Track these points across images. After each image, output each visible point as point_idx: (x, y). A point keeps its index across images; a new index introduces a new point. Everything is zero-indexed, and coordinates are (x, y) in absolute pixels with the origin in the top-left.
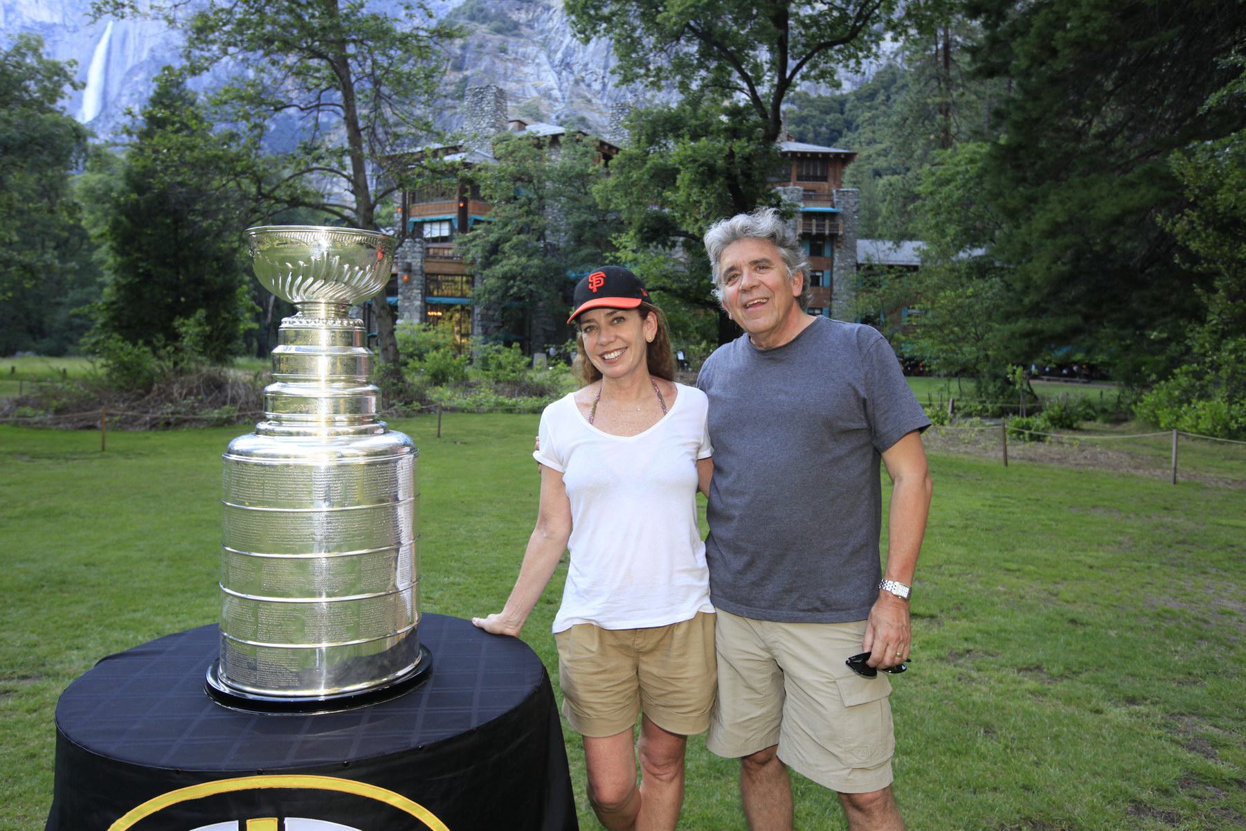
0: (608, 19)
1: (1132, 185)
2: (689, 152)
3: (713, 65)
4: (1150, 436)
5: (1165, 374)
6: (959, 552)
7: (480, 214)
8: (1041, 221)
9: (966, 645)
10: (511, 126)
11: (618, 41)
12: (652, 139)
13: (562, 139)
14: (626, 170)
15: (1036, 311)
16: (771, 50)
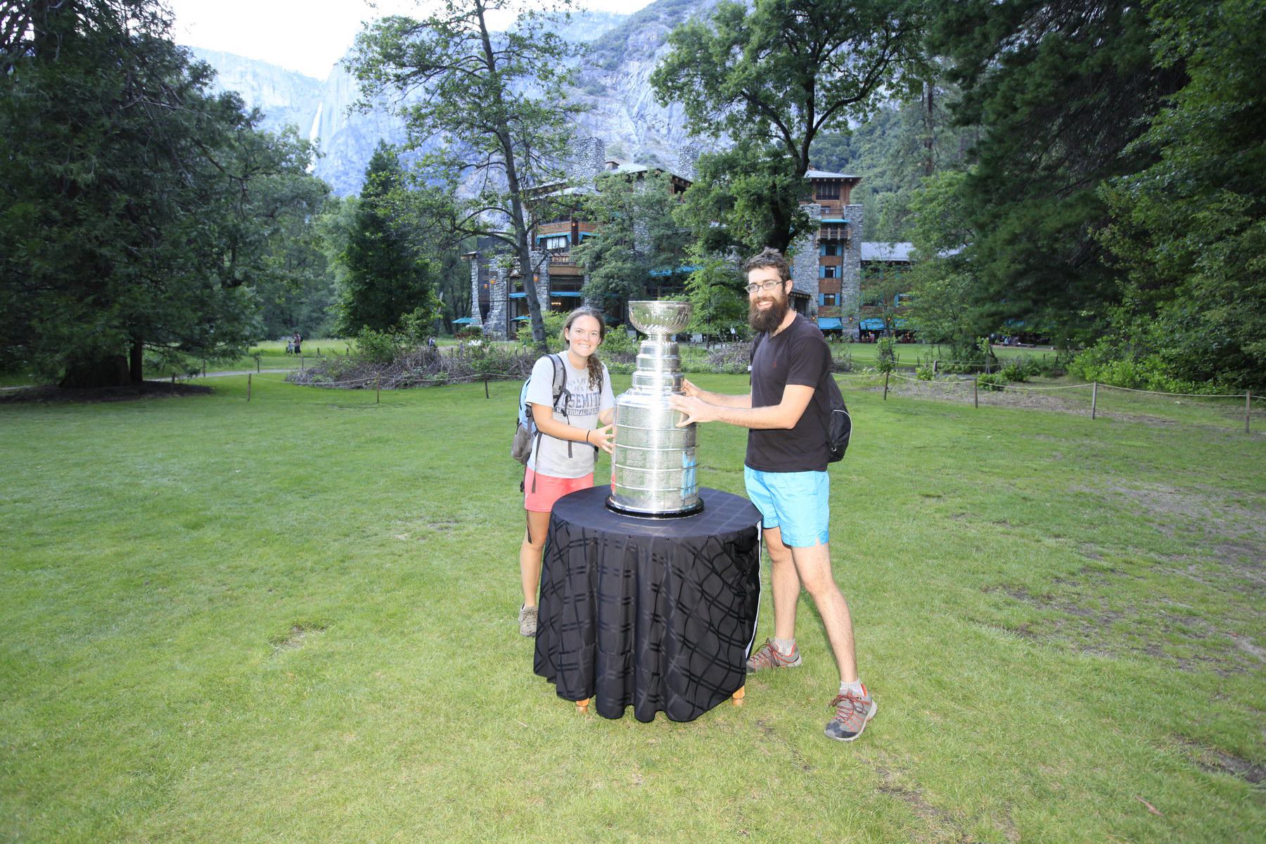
0: (681, 89)
1: (1071, 206)
2: (743, 185)
3: (758, 119)
4: (1079, 386)
5: (1090, 342)
6: (950, 461)
8: (1003, 233)
9: (961, 511)
10: (607, 166)
11: (688, 104)
12: (715, 176)
13: (645, 175)
14: (696, 198)
16: (800, 109)
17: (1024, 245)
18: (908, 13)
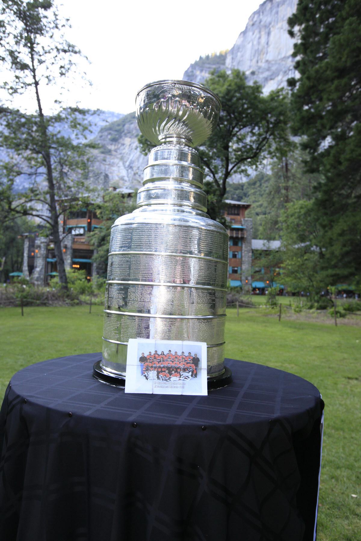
6: (346, 356)
7: (97, 225)
8: (337, 229)
15: (335, 266)
16: (222, 160)
17: (347, 237)
18: (281, 114)
